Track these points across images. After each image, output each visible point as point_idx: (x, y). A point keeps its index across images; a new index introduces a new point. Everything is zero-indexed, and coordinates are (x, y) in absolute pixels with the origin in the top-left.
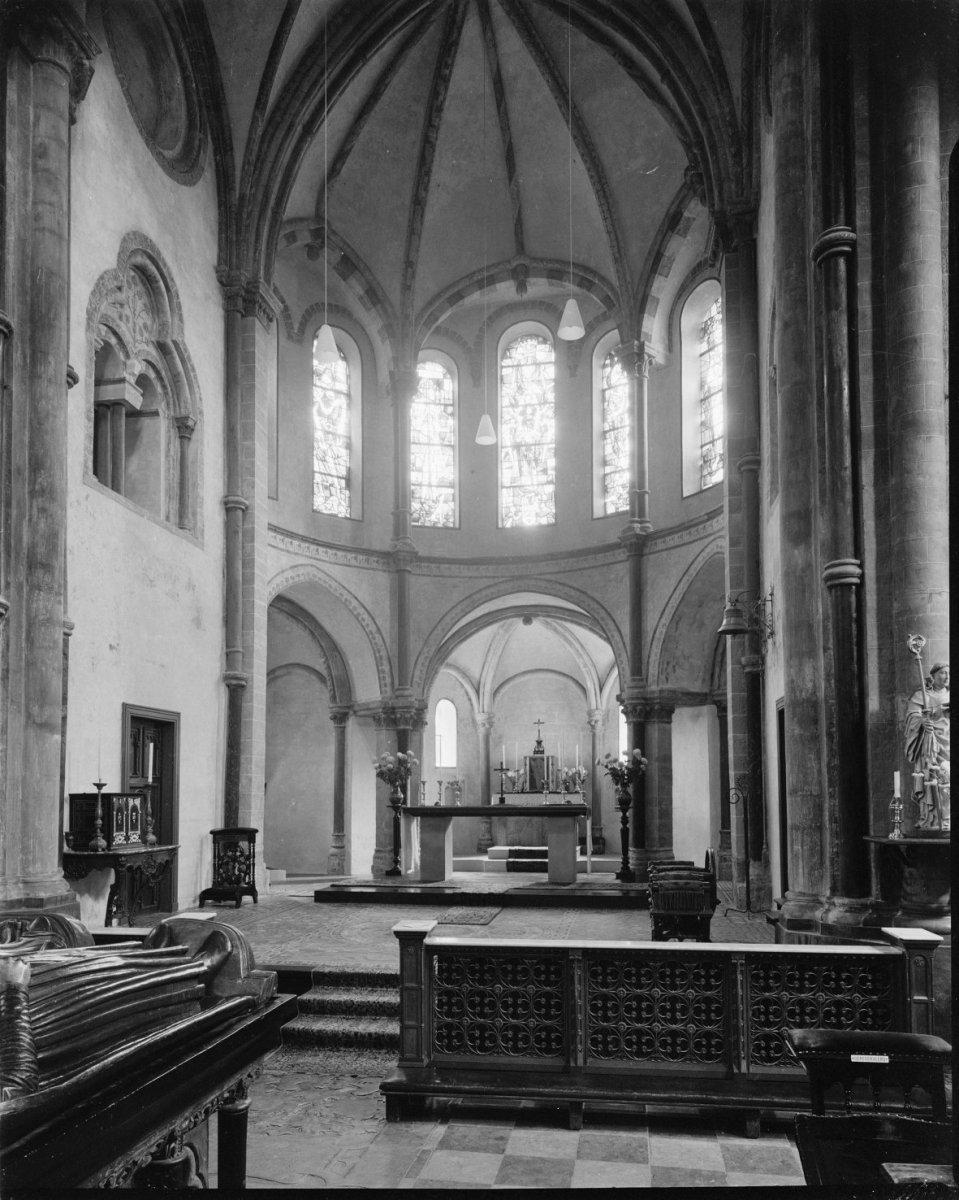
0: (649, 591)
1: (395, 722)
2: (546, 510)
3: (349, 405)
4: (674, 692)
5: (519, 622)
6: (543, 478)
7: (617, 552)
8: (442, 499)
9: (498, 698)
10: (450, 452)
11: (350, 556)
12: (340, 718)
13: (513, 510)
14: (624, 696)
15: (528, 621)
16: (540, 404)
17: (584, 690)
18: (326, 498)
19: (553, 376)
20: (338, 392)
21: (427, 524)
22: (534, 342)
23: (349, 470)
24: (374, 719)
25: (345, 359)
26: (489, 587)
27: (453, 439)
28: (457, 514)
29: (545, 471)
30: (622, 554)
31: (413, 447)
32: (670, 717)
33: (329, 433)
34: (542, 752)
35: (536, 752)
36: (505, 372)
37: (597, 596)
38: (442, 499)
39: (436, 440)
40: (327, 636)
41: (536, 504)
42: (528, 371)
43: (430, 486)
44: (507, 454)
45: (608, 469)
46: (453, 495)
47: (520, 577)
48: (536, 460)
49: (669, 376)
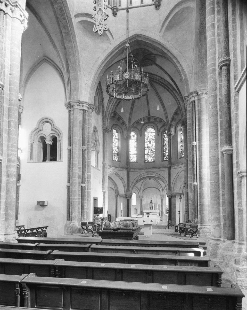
0: (171, 175)
1: (127, 197)
2: (153, 159)
3: (118, 141)
4: (176, 193)
5: (148, 179)
6: (153, 153)
7: (166, 168)
8: (134, 157)
9: (144, 192)
10: (136, 148)
11: (120, 169)
12: (117, 197)
13: (147, 159)
14: (168, 194)
15: (150, 179)
16: (152, 140)
17: (160, 191)
18: (114, 158)
19: (154, 135)
20: (116, 139)
21: (132, 161)
22: (151, 128)
23: (118, 152)
24: (123, 197)
25: (117, 133)
26: (143, 173)
27: (136, 146)
28: (137, 159)
29: (153, 152)
30: (167, 169)
31: (130, 148)
32: (175, 197)
33: (114, 146)
34: (152, 202)
35: (151, 202)
36: (146, 134)
37: (163, 176)
38: (134, 157)
39: (134, 146)
40: (114, 182)
41: (151, 158)
42: (150, 134)
43: (132, 154)
44: (146, 149)
45: (164, 152)
46: (136, 156)
47: (149, 172)
48: (151, 150)
49: (176, 136)
